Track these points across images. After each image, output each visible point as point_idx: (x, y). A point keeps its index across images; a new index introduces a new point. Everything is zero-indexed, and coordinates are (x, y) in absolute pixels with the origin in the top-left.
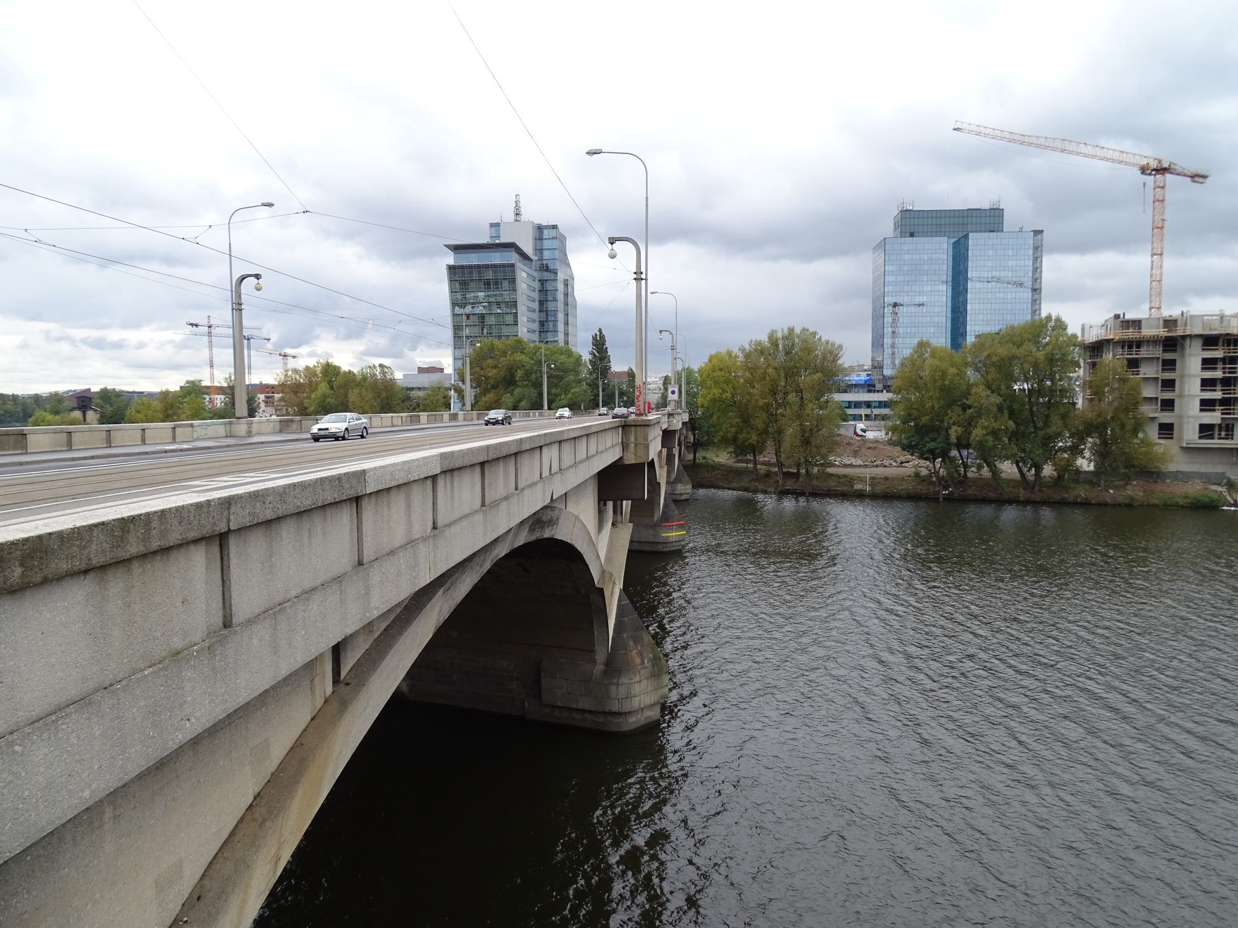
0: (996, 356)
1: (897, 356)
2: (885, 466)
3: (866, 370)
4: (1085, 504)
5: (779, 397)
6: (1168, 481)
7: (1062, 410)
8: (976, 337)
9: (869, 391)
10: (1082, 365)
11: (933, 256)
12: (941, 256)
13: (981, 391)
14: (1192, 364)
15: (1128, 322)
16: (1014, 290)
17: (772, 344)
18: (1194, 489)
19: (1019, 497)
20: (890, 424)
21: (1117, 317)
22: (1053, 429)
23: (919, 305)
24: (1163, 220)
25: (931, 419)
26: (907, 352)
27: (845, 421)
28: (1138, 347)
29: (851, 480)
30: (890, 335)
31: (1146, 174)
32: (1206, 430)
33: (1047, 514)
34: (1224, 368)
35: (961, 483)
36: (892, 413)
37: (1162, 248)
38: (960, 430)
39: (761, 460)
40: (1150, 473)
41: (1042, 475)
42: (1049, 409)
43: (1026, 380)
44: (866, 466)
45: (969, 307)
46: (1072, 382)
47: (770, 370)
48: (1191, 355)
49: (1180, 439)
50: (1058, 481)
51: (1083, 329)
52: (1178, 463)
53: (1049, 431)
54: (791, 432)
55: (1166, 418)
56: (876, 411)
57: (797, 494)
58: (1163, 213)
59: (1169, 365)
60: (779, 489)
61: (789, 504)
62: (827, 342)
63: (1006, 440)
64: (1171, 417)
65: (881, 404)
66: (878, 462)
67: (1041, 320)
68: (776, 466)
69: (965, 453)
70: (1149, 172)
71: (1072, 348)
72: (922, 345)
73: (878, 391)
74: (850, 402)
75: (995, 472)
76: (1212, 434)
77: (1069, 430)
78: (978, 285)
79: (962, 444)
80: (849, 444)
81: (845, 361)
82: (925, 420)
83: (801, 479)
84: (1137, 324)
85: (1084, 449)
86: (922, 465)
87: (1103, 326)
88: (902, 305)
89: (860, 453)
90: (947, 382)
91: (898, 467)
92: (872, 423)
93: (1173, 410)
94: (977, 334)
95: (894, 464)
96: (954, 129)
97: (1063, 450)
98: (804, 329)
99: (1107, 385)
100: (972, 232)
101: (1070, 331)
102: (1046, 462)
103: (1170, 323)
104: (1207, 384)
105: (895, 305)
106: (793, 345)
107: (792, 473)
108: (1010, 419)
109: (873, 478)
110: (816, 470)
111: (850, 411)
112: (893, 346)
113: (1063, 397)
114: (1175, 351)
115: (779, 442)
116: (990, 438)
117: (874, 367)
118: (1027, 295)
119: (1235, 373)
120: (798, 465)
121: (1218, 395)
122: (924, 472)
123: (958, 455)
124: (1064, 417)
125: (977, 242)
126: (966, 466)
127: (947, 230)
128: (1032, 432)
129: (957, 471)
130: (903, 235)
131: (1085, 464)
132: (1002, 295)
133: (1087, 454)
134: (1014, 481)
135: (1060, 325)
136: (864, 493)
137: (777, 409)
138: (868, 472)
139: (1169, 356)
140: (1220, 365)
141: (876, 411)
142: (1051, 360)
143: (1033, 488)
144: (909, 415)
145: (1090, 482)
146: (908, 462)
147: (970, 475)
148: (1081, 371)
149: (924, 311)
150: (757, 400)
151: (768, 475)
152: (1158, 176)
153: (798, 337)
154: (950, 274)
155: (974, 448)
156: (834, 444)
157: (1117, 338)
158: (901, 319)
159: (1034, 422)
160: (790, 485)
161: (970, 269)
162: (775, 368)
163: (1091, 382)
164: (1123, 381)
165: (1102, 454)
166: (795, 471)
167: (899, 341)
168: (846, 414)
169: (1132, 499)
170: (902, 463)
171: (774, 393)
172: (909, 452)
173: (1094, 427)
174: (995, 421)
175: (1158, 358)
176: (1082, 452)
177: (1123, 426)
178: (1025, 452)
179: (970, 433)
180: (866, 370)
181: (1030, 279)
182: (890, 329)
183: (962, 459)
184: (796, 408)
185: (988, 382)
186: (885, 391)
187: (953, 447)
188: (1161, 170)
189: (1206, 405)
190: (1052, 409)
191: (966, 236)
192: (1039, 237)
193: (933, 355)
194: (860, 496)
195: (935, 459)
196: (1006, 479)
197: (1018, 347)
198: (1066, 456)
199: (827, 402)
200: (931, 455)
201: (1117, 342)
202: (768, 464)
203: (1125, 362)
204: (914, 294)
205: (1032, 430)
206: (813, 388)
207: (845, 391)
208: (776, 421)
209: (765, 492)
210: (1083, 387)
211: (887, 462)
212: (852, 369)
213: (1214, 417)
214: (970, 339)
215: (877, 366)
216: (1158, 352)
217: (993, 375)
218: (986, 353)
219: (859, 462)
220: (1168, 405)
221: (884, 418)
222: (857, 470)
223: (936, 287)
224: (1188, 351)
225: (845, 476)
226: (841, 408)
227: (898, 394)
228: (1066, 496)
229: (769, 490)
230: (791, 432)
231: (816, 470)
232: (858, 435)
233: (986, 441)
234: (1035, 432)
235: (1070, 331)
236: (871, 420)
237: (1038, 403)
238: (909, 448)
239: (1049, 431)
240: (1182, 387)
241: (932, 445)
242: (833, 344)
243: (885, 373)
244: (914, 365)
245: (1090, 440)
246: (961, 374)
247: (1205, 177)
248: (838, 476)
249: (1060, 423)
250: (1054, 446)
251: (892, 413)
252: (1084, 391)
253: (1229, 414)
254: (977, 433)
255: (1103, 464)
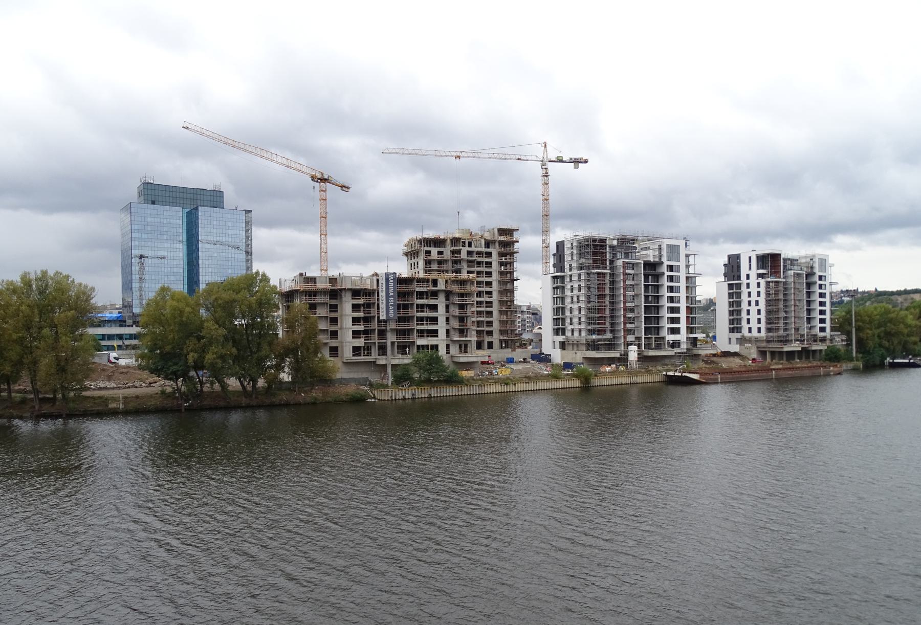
0: (221, 299)
1: (144, 297)
2: (136, 387)
3: (117, 309)
4: (287, 405)
5: (34, 330)
6: (337, 385)
7: (269, 339)
8: (207, 285)
9: (121, 326)
10: (281, 307)
11: (171, 220)
12: (178, 221)
13: (211, 325)
14: (347, 306)
15: (308, 278)
16: (233, 251)
17: (25, 284)
18: (351, 389)
19: (241, 404)
20: (140, 352)
21: (301, 275)
22: (263, 353)
23: (161, 258)
24: (326, 213)
25: (173, 348)
26: (152, 295)
27: (99, 351)
28: (315, 295)
29: (105, 400)
30: (138, 281)
31: (315, 181)
32: (356, 350)
33: (262, 414)
34: (364, 311)
35: (198, 396)
36: (140, 343)
37: (326, 230)
38: (196, 355)
39: (16, 388)
40: (325, 380)
41: (257, 386)
42: (260, 338)
43: (243, 317)
44: (119, 388)
45: (200, 262)
46: (275, 319)
47: (23, 308)
48: (345, 301)
49: (342, 357)
50: (268, 390)
51: (280, 283)
52: (342, 373)
53: (260, 354)
54: (46, 362)
55: (333, 343)
56: (127, 342)
57: (53, 416)
58: (326, 207)
59: (334, 308)
60: (36, 413)
61: (46, 426)
62: (80, 285)
63: (231, 361)
64: (336, 342)
65: (132, 337)
66: (130, 384)
67: (252, 274)
68: (32, 393)
69: (201, 373)
70: (316, 180)
71: (273, 295)
72: (163, 290)
73: (129, 326)
74: (103, 335)
75: (224, 386)
76: (360, 353)
77: (274, 353)
78: (207, 246)
79: (198, 366)
80: (103, 370)
81: (98, 300)
82: (168, 348)
83: (58, 403)
84: (313, 280)
85: (285, 366)
86: (167, 384)
87: (293, 280)
88: (147, 257)
89: (114, 377)
90: (184, 319)
91: (147, 387)
92: (124, 352)
93: (337, 338)
94: (207, 282)
95: (144, 385)
96: (183, 127)
97: (270, 367)
98: (57, 272)
99: (297, 321)
100: (200, 206)
101: (272, 283)
102: (260, 377)
103: (333, 280)
104: (356, 320)
105: (141, 257)
106: (47, 285)
107: (48, 398)
108: (233, 346)
109: (125, 398)
110: (72, 394)
111: (103, 343)
112: (140, 289)
113: (269, 329)
114: (336, 299)
115: (35, 371)
116: (219, 361)
117: (124, 306)
118: (243, 256)
119: (370, 313)
120: (55, 391)
121: (361, 328)
122: (169, 390)
123: (195, 375)
124: (270, 344)
125: (204, 213)
126: (201, 383)
127: (182, 202)
128: (249, 356)
129: (195, 387)
130: (145, 201)
131: (285, 377)
132: (224, 254)
133: (286, 369)
134: (238, 392)
135: (265, 279)
136: (118, 410)
137: (31, 342)
138: (121, 393)
139: (333, 302)
140: (362, 309)
141: (127, 342)
142: (260, 304)
143: (251, 396)
144: (155, 344)
145: (289, 389)
146: (156, 382)
147: (205, 389)
148: (280, 312)
149: (166, 263)
150: (10, 335)
151: (24, 401)
152: (322, 184)
153: (52, 279)
154: (185, 235)
155: (208, 370)
156: (89, 371)
157: (302, 289)
158: (146, 269)
159: (250, 348)
160: (46, 409)
161: (200, 233)
162: (29, 306)
163: (286, 319)
164: (307, 318)
165: (296, 370)
166: (52, 396)
167: (146, 285)
168: (100, 345)
169: (316, 399)
170: (150, 383)
171: (28, 328)
172: (156, 374)
173: (290, 351)
174: (223, 348)
175: (327, 303)
176: (283, 368)
177: (308, 349)
178: (244, 370)
179: (204, 358)
180: (117, 309)
181: (244, 244)
182: (138, 276)
183: (199, 378)
184: (50, 341)
185: (215, 318)
186: (134, 326)
187: (191, 369)
188: (324, 180)
189: (356, 334)
190: (262, 338)
191: (197, 209)
192: (249, 215)
193: (172, 298)
194: (114, 414)
195: (177, 379)
196: (231, 391)
197: (237, 293)
198: (273, 371)
199: (81, 335)
200: (174, 376)
201: (302, 292)
202: (24, 391)
203: (308, 306)
204: (156, 249)
205: (249, 354)
206: (67, 323)
207: (99, 326)
208: (31, 353)
209: (21, 418)
210: (282, 323)
211: (137, 384)
212: (104, 308)
213: (360, 342)
214: (202, 286)
215: (127, 306)
216: (326, 299)
217: (220, 313)
218: (214, 297)
219: (113, 385)
220: (334, 334)
221: (134, 347)
222: (111, 392)
223: (175, 245)
224: (344, 299)
225: (100, 398)
226: (95, 340)
227: (145, 328)
228: (274, 400)
229: (25, 415)
230: (46, 362)
231: (72, 394)
232: (111, 363)
233: (216, 363)
234: (251, 355)
235: (272, 283)
236: (123, 350)
237: (253, 334)
238: (155, 371)
239: (260, 354)
240: (341, 323)
241: (175, 368)
242: (86, 287)
243: (134, 311)
244: (157, 304)
245: (288, 359)
246: (195, 312)
247: (348, 188)
248: (93, 398)
249: (267, 348)
250: (265, 365)
251: (140, 343)
252: (283, 325)
253: (368, 340)
254: (209, 357)
255: (297, 376)
